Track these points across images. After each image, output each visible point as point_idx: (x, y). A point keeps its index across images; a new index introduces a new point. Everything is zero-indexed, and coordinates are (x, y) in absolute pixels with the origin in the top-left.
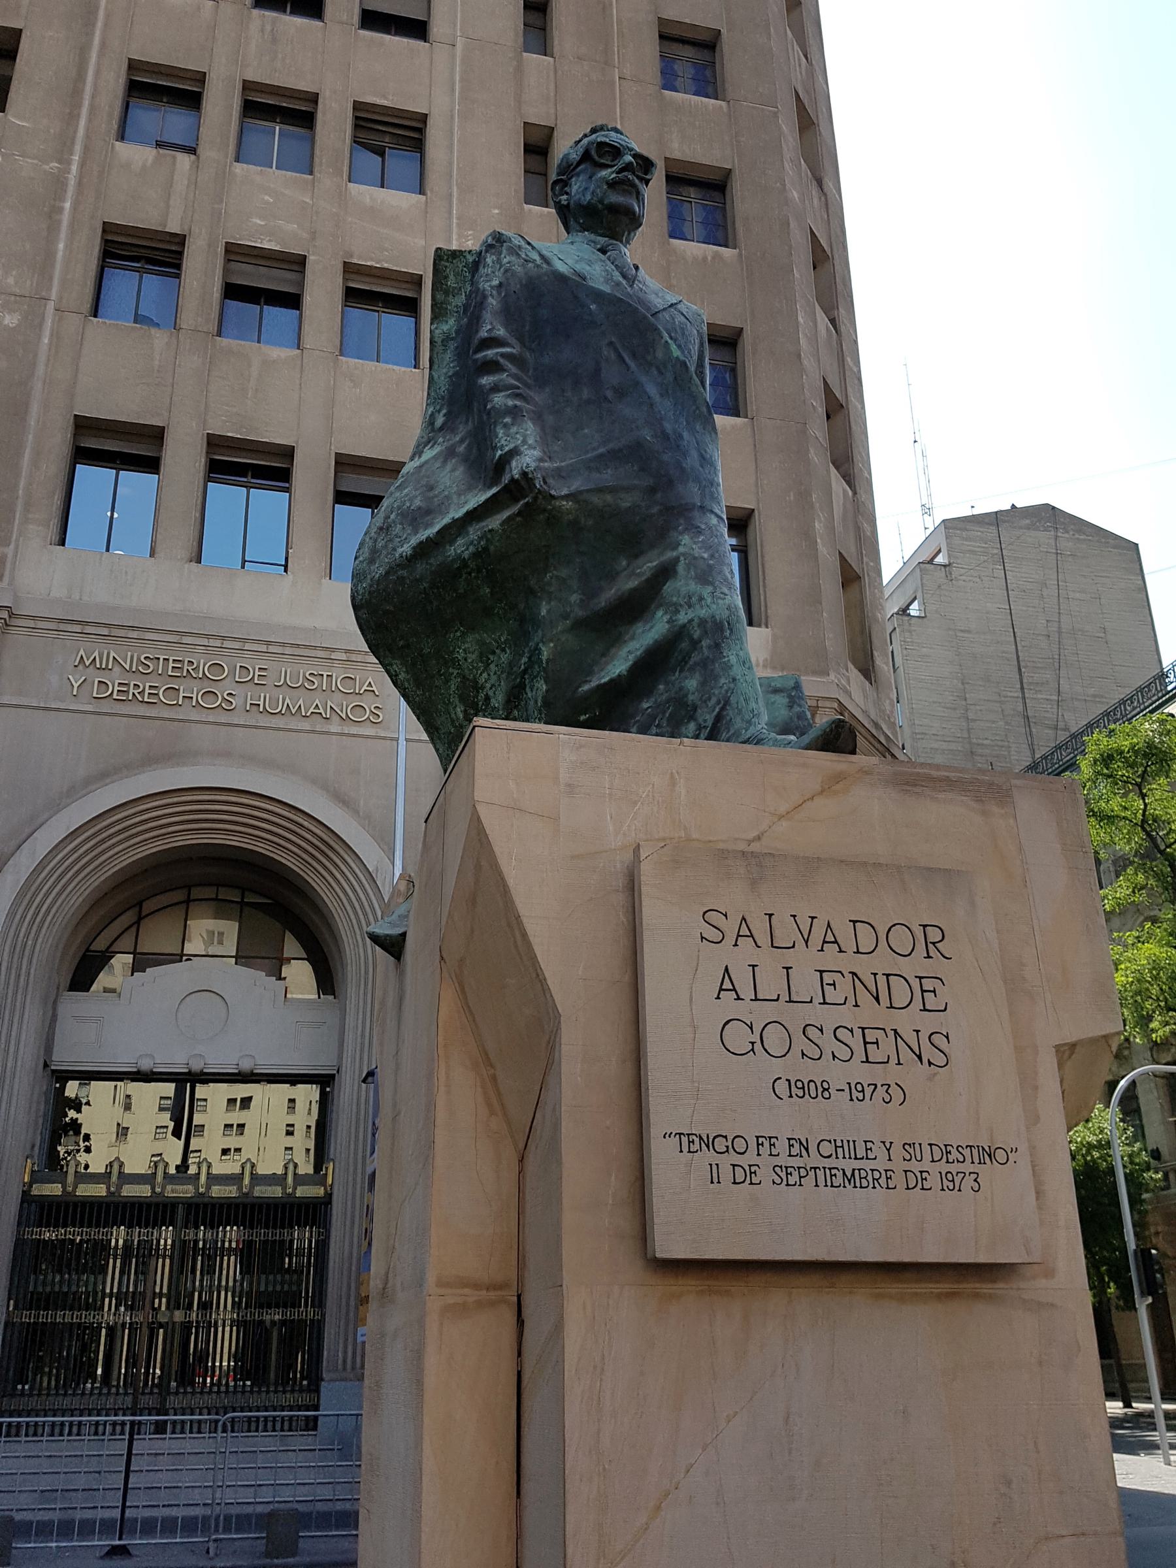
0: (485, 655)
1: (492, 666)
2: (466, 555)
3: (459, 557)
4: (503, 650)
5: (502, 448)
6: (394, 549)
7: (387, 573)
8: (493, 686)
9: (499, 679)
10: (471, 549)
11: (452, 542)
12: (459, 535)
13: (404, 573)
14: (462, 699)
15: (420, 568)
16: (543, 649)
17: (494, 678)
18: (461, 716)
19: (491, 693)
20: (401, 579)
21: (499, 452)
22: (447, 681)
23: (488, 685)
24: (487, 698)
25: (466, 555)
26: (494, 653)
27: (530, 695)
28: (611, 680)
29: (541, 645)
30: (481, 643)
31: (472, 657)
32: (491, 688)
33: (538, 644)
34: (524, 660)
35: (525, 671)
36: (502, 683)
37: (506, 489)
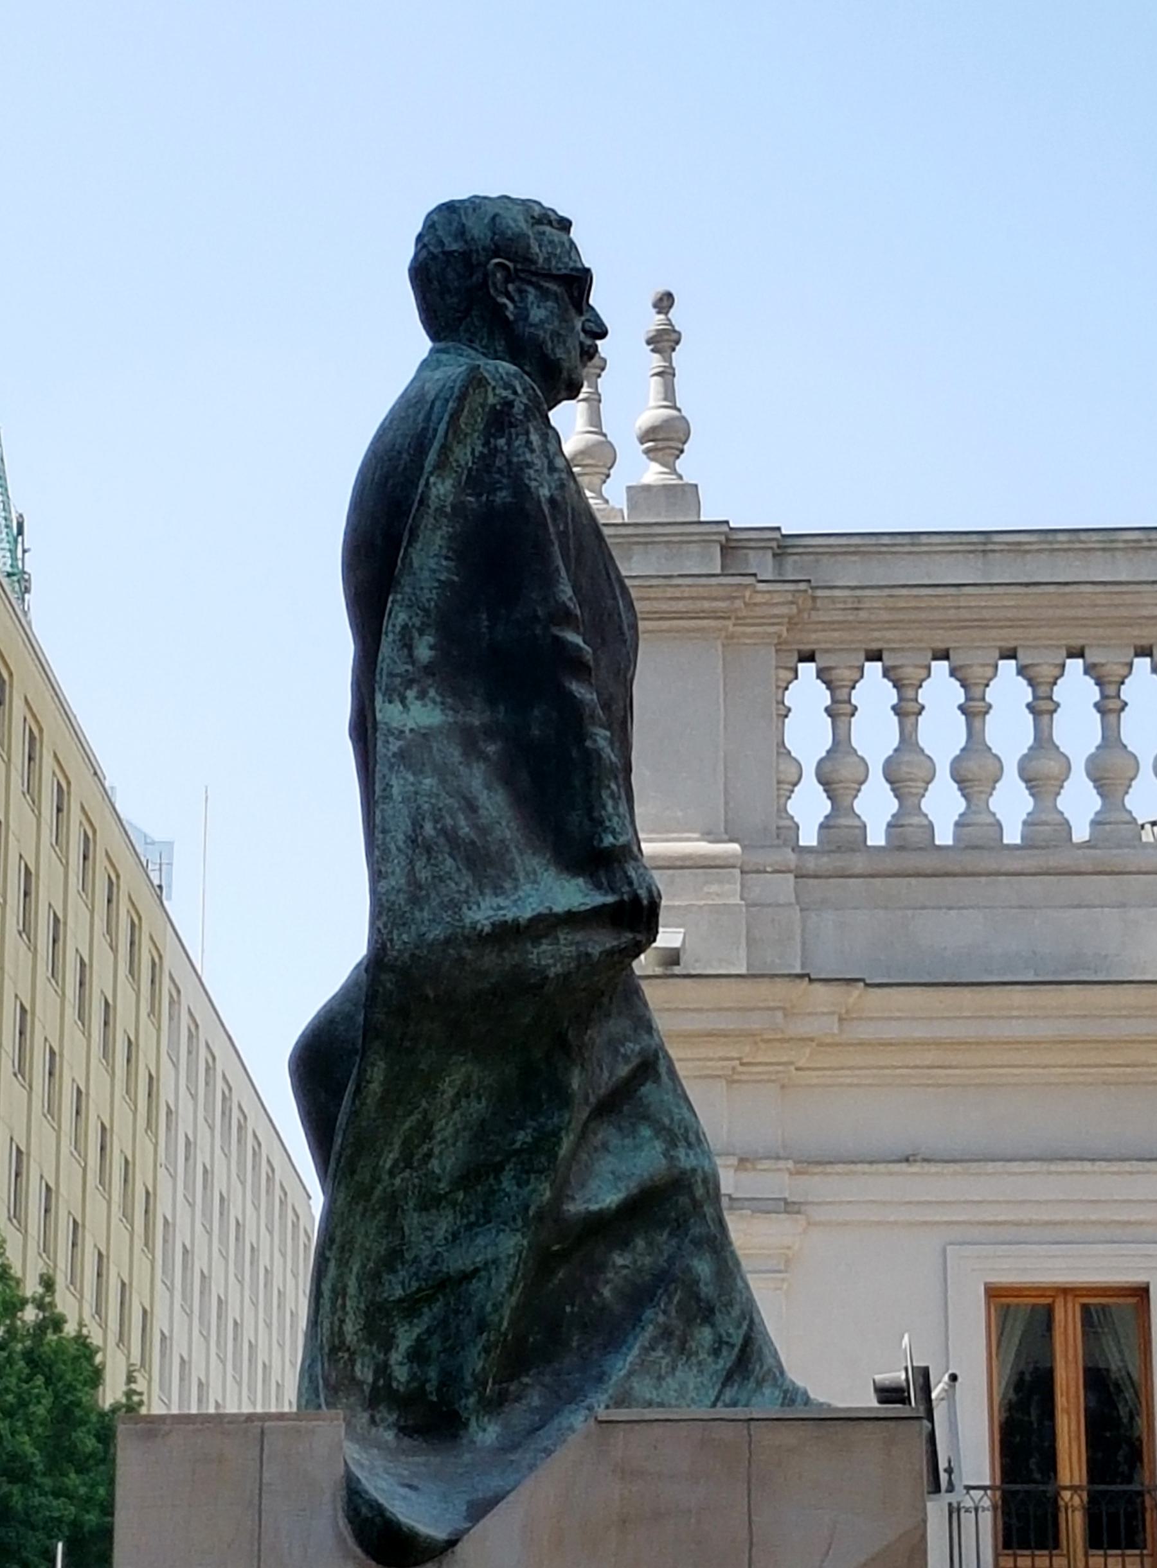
0: (464, 1093)
1: (456, 1114)
2: (552, 972)
3: (541, 971)
4: (479, 1098)
5: (614, 833)
6: (454, 906)
7: (448, 941)
8: (444, 1141)
9: (457, 1132)
10: (559, 969)
11: (536, 940)
12: (546, 936)
13: (467, 953)
14: (405, 1143)
15: (490, 960)
16: (565, 1139)
17: (450, 1130)
18: (388, 1165)
19: (436, 1151)
20: (461, 960)
21: (608, 840)
22: (411, 1113)
23: (439, 1138)
24: (429, 1155)
25: (552, 972)
26: (468, 1096)
27: (508, 1185)
28: (601, 1210)
29: (563, 1133)
30: (468, 1079)
31: (451, 1093)
32: (441, 1143)
33: (561, 1129)
34: (523, 1137)
35: (517, 1152)
36: (460, 1144)
37: (619, 905)
